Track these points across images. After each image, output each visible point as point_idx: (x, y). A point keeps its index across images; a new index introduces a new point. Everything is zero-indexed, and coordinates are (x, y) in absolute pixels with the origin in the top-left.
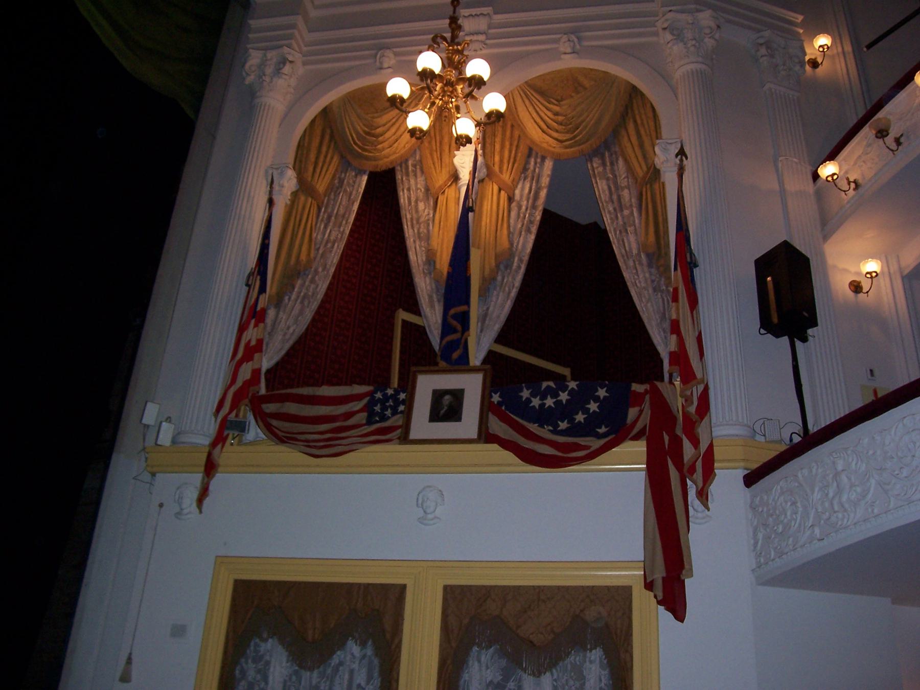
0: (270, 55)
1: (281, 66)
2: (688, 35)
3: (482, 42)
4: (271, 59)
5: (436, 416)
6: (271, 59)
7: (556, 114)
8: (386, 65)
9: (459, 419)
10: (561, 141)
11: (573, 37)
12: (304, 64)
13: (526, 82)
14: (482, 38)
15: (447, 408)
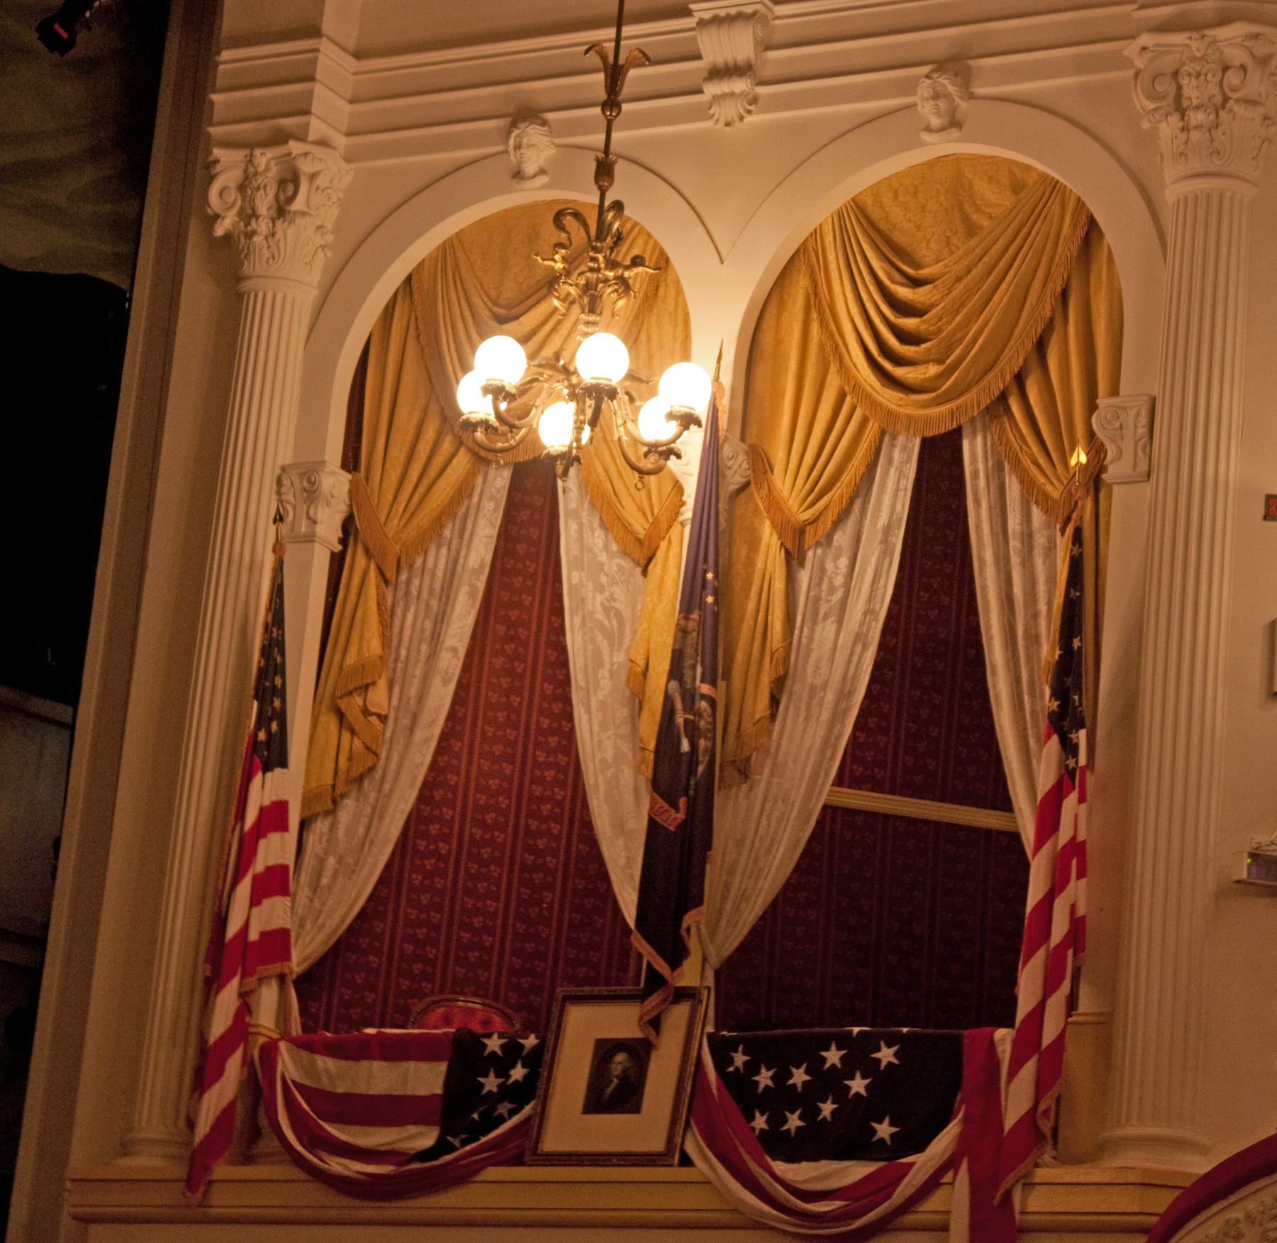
0: (264, 158)
1: (290, 188)
2: (1192, 93)
4: (267, 169)
5: (597, 1102)
6: (267, 169)
8: (530, 168)
9: (636, 1109)
11: (946, 83)
14: (739, 85)
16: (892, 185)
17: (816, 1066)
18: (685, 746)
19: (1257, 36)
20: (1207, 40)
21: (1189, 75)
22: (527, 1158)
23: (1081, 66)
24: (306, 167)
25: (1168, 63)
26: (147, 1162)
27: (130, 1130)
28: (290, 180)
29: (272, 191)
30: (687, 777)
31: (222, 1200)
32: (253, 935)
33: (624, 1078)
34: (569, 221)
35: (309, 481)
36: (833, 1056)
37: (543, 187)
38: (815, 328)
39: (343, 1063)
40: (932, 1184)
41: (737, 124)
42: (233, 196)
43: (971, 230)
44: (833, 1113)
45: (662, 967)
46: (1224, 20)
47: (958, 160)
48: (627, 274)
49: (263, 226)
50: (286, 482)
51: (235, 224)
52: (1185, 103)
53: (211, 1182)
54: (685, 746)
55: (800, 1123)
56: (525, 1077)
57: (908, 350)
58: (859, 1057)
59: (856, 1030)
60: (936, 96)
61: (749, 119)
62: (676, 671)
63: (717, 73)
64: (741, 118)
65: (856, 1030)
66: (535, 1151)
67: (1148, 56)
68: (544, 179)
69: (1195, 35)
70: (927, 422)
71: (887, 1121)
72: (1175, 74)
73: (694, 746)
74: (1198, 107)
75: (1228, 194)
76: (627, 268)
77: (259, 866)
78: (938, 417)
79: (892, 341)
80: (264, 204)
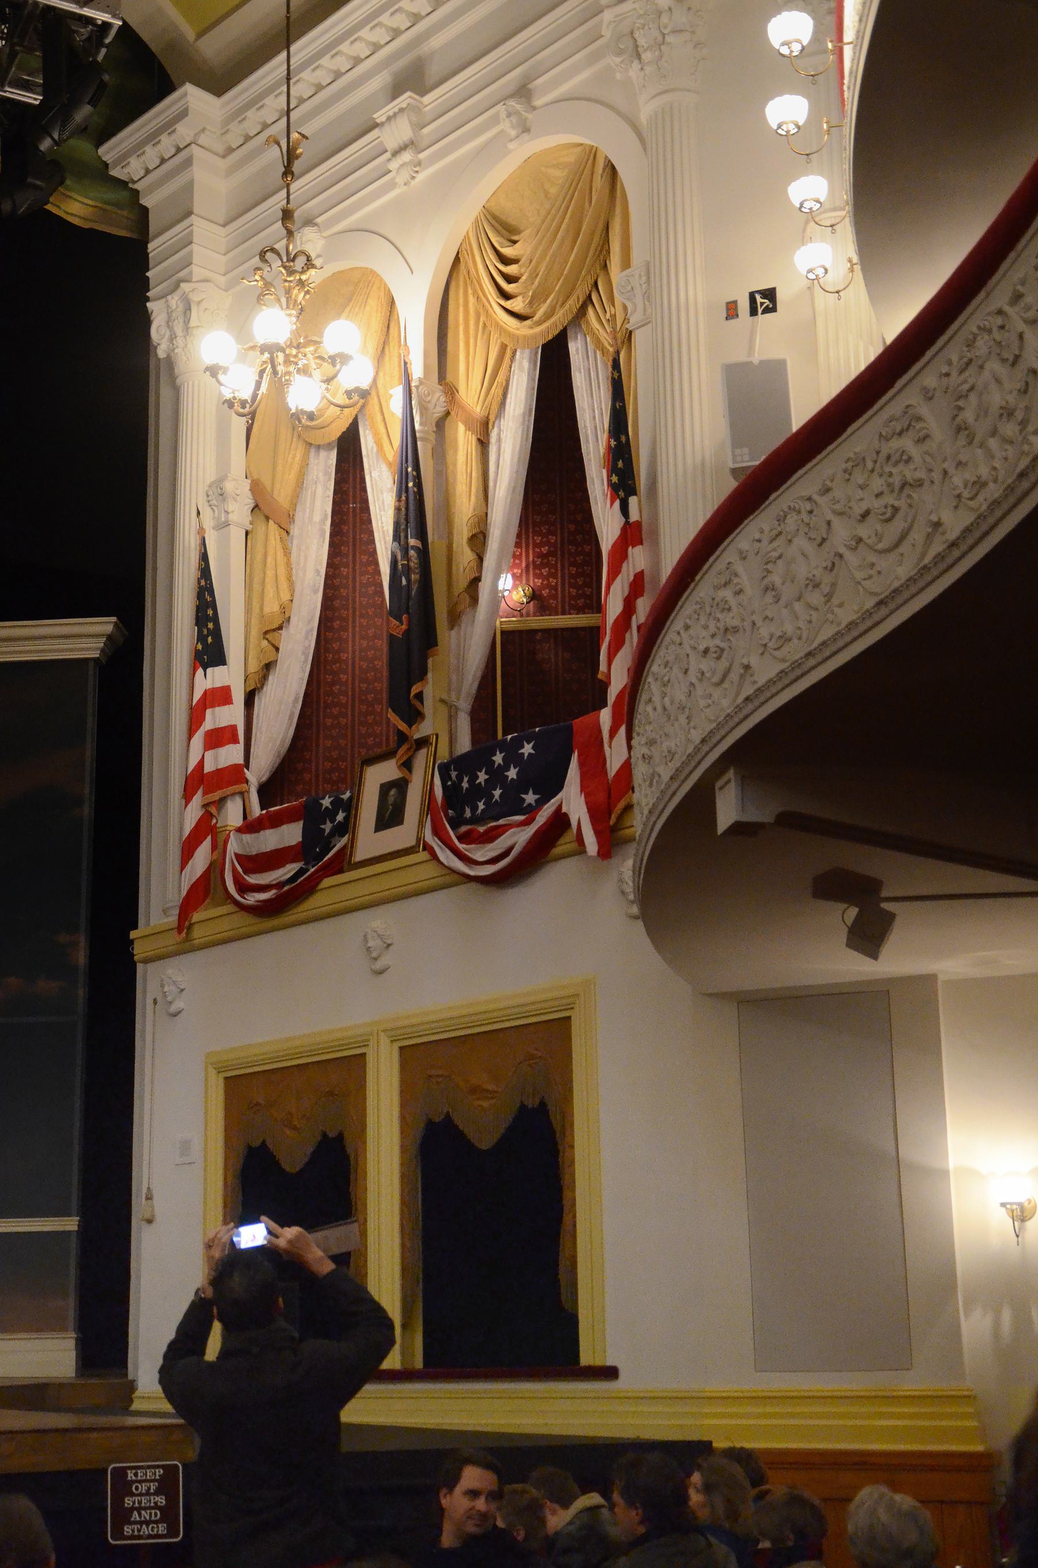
18: (404, 582)
31: (199, 934)
32: (208, 768)
33: (394, 805)
34: (269, 256)
36: (498, 758)
38: (472, 300)
39: (253, 835)
44: (501, 796)
45: (402, 726)
48: (304, 277)
54: (404, 582)
56: (344, 818)
59: (509, 737)
61: (421, 177)
62: (396, 537)
63: (396, 153)
70: (534, 337)
71: (531, 791)
72: (632, 33)
73: (409, 580)
76: (303, 272)
77: (208, 725)
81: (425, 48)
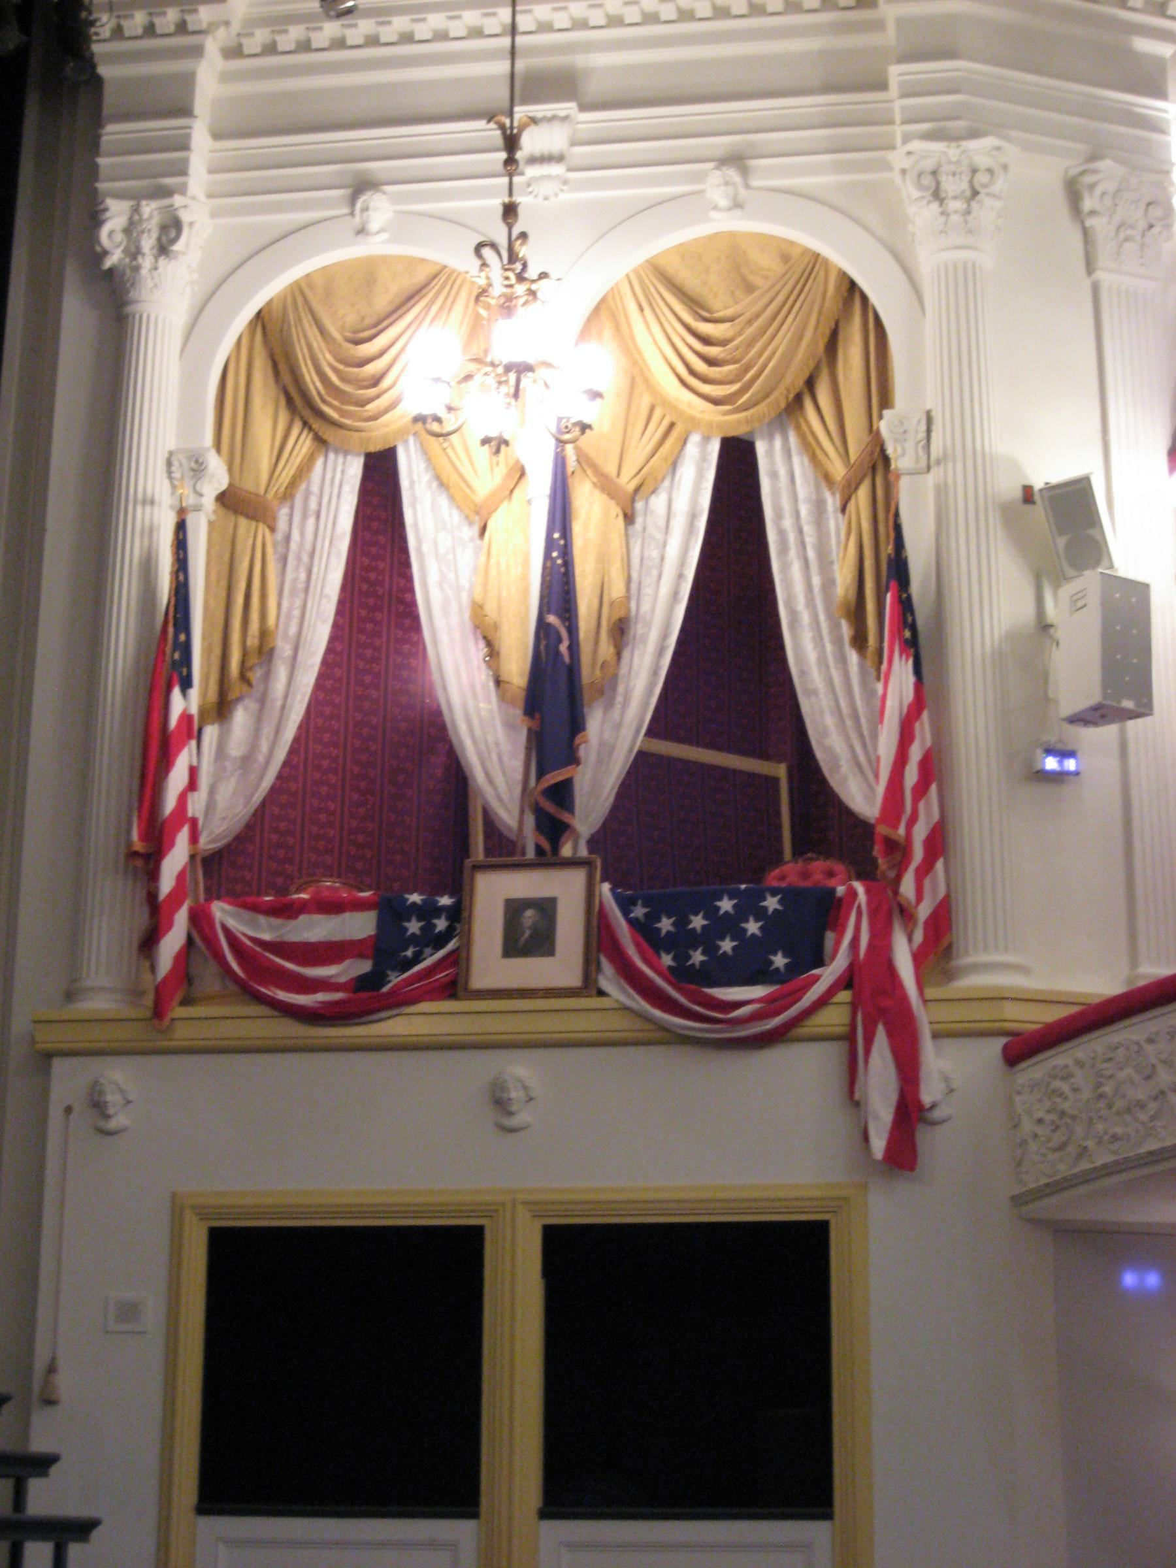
0: (149, 208)
1: (173, 234)
2: (950, 186)
3: (558, 177)
4: (151, 217)
5: (514, 946)
6: (151, 217)
7: (706, 340)
8: (374, 226)
9: (550, 952)
10: (716, 402)
11: (732, 174)
12: (214, 215)
13: (647, 261)
15: (529, 933)
16: (683, 251)
17: (712, 913)
19: (999, 149)
20: (962, 148)
21: (947, 174)
22: (461, 994)
23: (838, 168)
24: (185, 216)
25: (928, 164)
26: (98, 1004)
27: (74, 981)
28: (172, 228)
29: (155, 235)
30: (554, 696)
31: (183, 1034)
33: (535, 929)
35: (197, 462)
37: (384, 242)
40: (823, 1001)
41: (552, 199)
42: (119, 237)
43: (750, 288)
46: (974, 134)
47: (732, 235)
49: (146, 262)
50: (176, 463)
51: (120, 260)
52: (943, 195)
53: (173, 1020)
55: (702, 958)
57: (713, 372)
58: (749, 906)
59: (743, 887)
60: (727, 184)
64: (556, 195)
65: (743, 887)
66: (466, 989)
67: (913, 158)
68: (384, 236)
69: (953, 144)
74: (955, 198)
75: (970, 265)
78: (734, 423)
79: (700, 366)
80: (148, 244)
81: (581, 60)
